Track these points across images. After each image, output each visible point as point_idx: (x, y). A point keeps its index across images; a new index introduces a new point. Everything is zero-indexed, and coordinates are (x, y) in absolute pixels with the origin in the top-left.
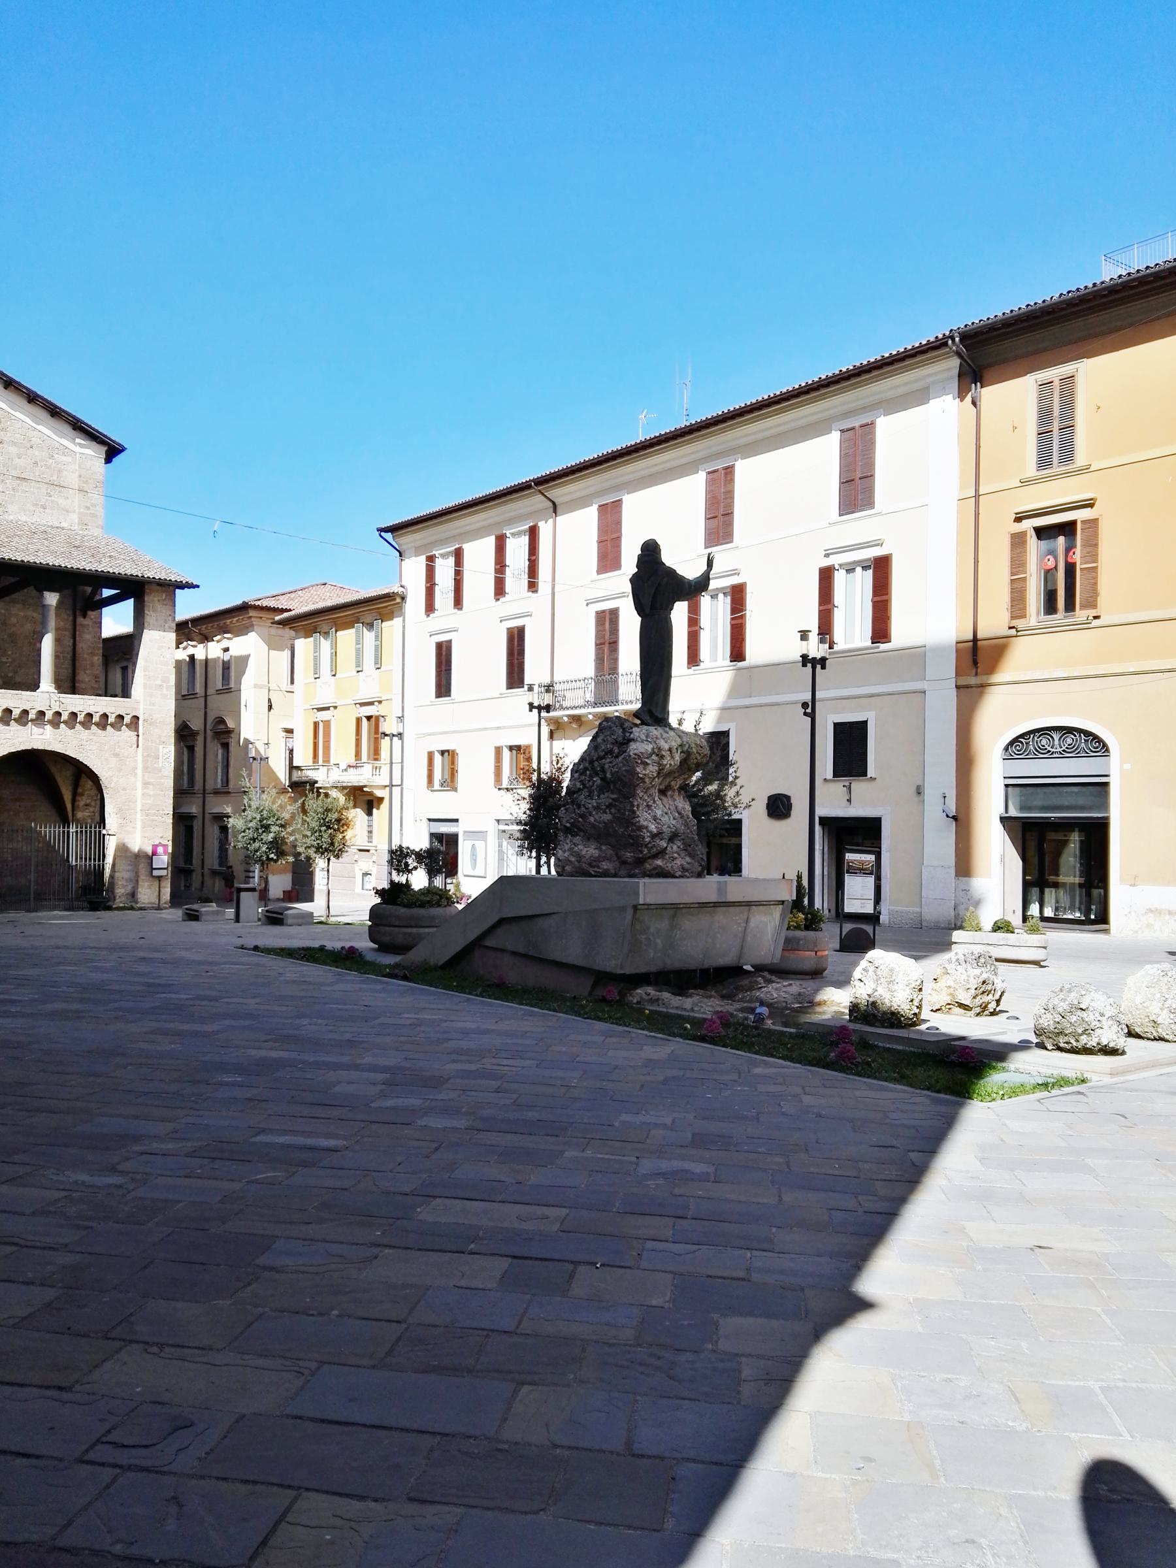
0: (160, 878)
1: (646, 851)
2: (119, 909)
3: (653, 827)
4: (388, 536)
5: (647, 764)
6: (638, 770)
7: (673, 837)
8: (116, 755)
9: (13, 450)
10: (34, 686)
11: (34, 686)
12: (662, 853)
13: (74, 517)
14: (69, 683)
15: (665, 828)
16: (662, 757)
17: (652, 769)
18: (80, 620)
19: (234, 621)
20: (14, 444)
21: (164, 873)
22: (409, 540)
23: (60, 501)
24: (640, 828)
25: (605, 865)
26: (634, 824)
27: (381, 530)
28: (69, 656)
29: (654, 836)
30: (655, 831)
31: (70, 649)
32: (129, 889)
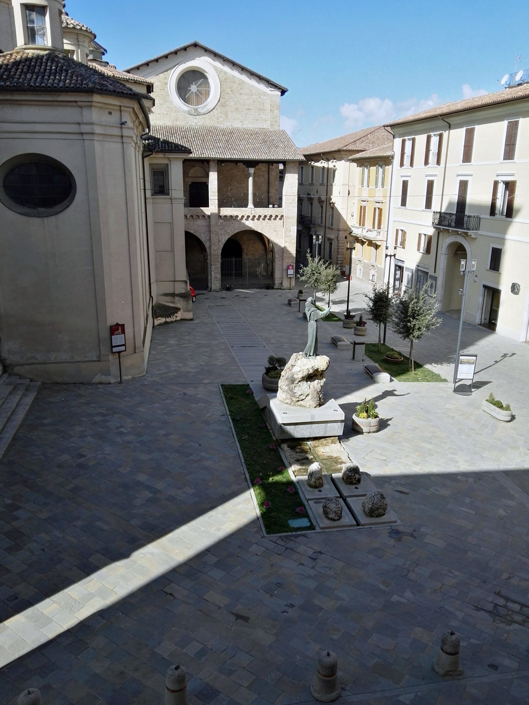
0: (290, 278)
2: (276, 289)
4: (389, 129)
8: (275, 231)
9: (245, 97)
10: (246, 206)
11: (246, 206)
13: (269, 122)
14: (257, 205)
18: (271, 167)
19: (336, 155)
20: (246, 94)
21: (292, 276)
22: (397, 130)
23: (264, 116)
28: (267, 182)
31: (267, 179)
32: (280, 281)
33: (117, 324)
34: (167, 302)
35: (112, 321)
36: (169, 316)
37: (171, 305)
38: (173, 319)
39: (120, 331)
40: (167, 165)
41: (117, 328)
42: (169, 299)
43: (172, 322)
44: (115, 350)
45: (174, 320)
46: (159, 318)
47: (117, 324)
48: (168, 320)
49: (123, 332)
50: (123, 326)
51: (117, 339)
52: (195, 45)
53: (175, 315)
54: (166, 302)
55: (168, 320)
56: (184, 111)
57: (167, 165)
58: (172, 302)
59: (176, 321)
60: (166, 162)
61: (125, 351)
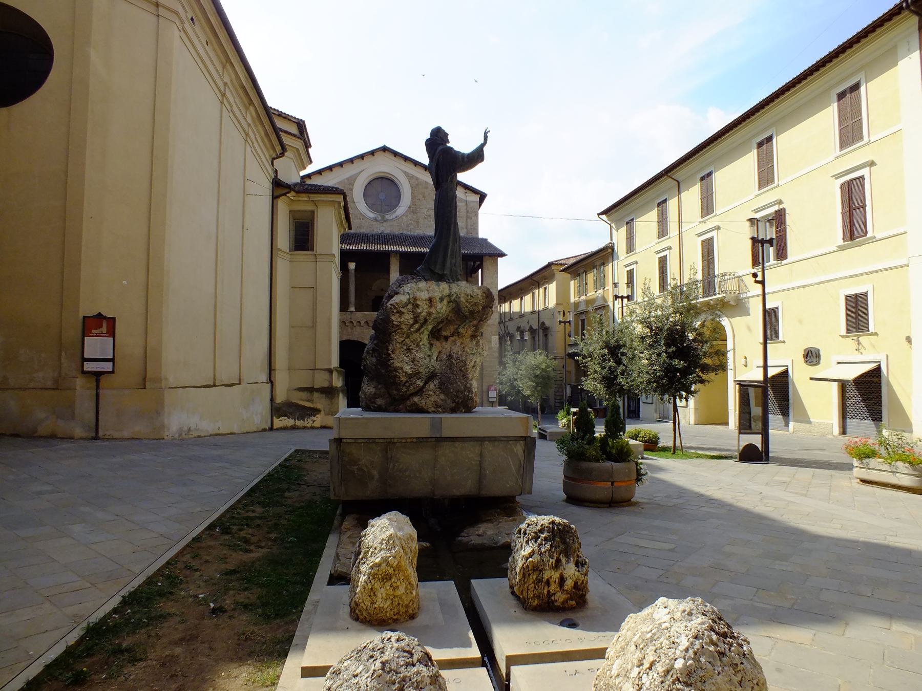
1: (404, 389)
3: (408, 369)
5: (403, 313)
6: (393, 318)
7: (431, 377)
12: (420, 391)
15: (421, 369)
16: (417, 306)
17: (408, 317)
24: (396, 369)
25: (380, 402)
26: (389, 366)
27: (599, 214)
29: (410, 376)
30: (410, 371)
33: (100, 314)
34: (302, 400)
35: (88, 308)
36: (302, 418)
37: (308, 404)
38: (308, 423)
39: (104, 329)
40: (313, 212)
41: (99, 323)
42: (304, 395)
43: (304, 428)
44: (89, 367)
45: (309, 425)
46: (283, 418)
47: (100, 314)
48: (299, 423)
49: (112, 333)
50: (112, 321)
51: (96, 346)
52: (385, 149)
53: (312, 418)
54: (300, 399)
55: (299, 423)
56: (369, 219)
57: (313, 212)
58: (309, 401)
59: (312, 428)
60: (309, 207)
61: (113, 372)
